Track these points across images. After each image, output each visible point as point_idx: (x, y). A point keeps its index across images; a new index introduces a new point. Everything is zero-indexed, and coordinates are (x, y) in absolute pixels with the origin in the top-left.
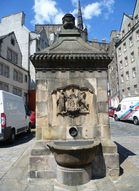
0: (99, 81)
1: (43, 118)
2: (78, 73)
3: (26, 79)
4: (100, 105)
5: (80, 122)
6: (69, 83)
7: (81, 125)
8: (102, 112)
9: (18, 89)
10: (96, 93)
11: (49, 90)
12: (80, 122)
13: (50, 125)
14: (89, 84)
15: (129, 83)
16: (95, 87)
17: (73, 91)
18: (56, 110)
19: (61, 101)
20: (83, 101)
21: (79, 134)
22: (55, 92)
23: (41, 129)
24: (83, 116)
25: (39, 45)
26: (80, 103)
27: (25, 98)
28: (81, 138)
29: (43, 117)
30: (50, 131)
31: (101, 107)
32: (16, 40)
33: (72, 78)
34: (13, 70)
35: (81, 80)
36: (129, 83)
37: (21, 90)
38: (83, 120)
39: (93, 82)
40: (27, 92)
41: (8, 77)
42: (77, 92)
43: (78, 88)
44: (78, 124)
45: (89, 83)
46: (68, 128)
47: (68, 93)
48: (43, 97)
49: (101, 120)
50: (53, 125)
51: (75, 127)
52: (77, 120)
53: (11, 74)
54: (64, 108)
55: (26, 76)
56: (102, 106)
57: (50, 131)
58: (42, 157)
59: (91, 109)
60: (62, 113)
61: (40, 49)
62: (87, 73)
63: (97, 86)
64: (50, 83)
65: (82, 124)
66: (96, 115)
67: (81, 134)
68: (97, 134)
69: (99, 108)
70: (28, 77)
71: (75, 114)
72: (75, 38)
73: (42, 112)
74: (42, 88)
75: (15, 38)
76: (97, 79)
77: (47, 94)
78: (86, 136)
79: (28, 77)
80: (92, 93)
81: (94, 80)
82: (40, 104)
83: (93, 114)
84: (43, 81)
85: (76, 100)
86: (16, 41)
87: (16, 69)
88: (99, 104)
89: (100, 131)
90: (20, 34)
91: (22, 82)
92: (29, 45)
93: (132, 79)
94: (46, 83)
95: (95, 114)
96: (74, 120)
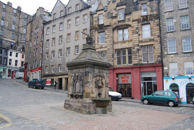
2: (101, 70)
6: (98, 74)
15: (54, 61)
18: (94, 86)
26: (102, 83)
28: (101, 97)
33: (99, 72)
36: (54, 61)
44: (100, 91)
48: (90, 80)
59: (104, 86)
72: (94, 51)
93: (57, 58)
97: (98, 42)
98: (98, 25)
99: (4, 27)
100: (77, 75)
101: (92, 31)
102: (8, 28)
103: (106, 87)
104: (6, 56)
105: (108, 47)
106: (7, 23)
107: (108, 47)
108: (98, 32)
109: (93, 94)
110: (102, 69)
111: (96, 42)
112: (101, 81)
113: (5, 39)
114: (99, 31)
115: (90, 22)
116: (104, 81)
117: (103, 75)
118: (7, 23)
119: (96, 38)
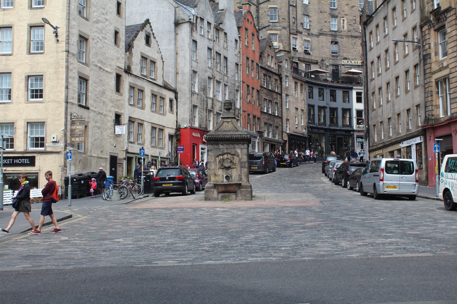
3: (171, 106)
5: (231, 172)
6: (226, 151)
8: (243, 167)
9: (158, 127)
10: (240, 157)
13: (215, 174)
16: (240, 154)
17: (228, 155)
18: (218, 166)
19: (222, 161)
20: (233, 161)
21: (231, 179)
22: (218, 156)
23: (210, 176)
24: (233, 169)
25: (194, 34)
27: (170, 143)
30: (215, 178)
31: (243, 165)
32: (153, 34)
34: (150, 94)
37: (162, 130)
38: (232, 172)
39: (239, 151)
40: (173, 132)
41: (143, 108)
42: (229, 156)
43: (230, 154)
46: (225, 176)
47: (225, 156)
49: (243, 172)
50: (217, 174)
52: (229, 171)
53: (148, 101)
54: (222, 165)
55: (171, 101)
58: (211, 190)
60: (222, 167)
61: (197, 40)
62: (236, 146)
63: (241, 153)
67: (232, 179)
68: (241, 179)
70: (175, 101)
71: (229, 168)
72: (230, 120)
75: (152, 30)
76: (241, 149)
77: (213, 158)
79: (175, 101)
80: (238, 157)
84: (211, 150)
85: (229, 161)
86: (152, 36)
87: (154, 90)
90: (155, 11)
91: (164, 114)
92: (176, 34)
97: (436, 54)
98: (431, 13)
99: (338, 33)
101: (424, 29)
102: (350, 34)
103: (241, 167)
104: (346, 106)
105: (451, 66)
106: (346, 22)
107: (451, 66)
108: (435, 31)
109: (217, 178)
110: (232, 144)
111: (433, 55)
113: (345, 62)
114: (437, 27)
115: (420, 7)
116: (236, 160)
117: (236, 152)
118: (346, 22)
119: (432, 46)
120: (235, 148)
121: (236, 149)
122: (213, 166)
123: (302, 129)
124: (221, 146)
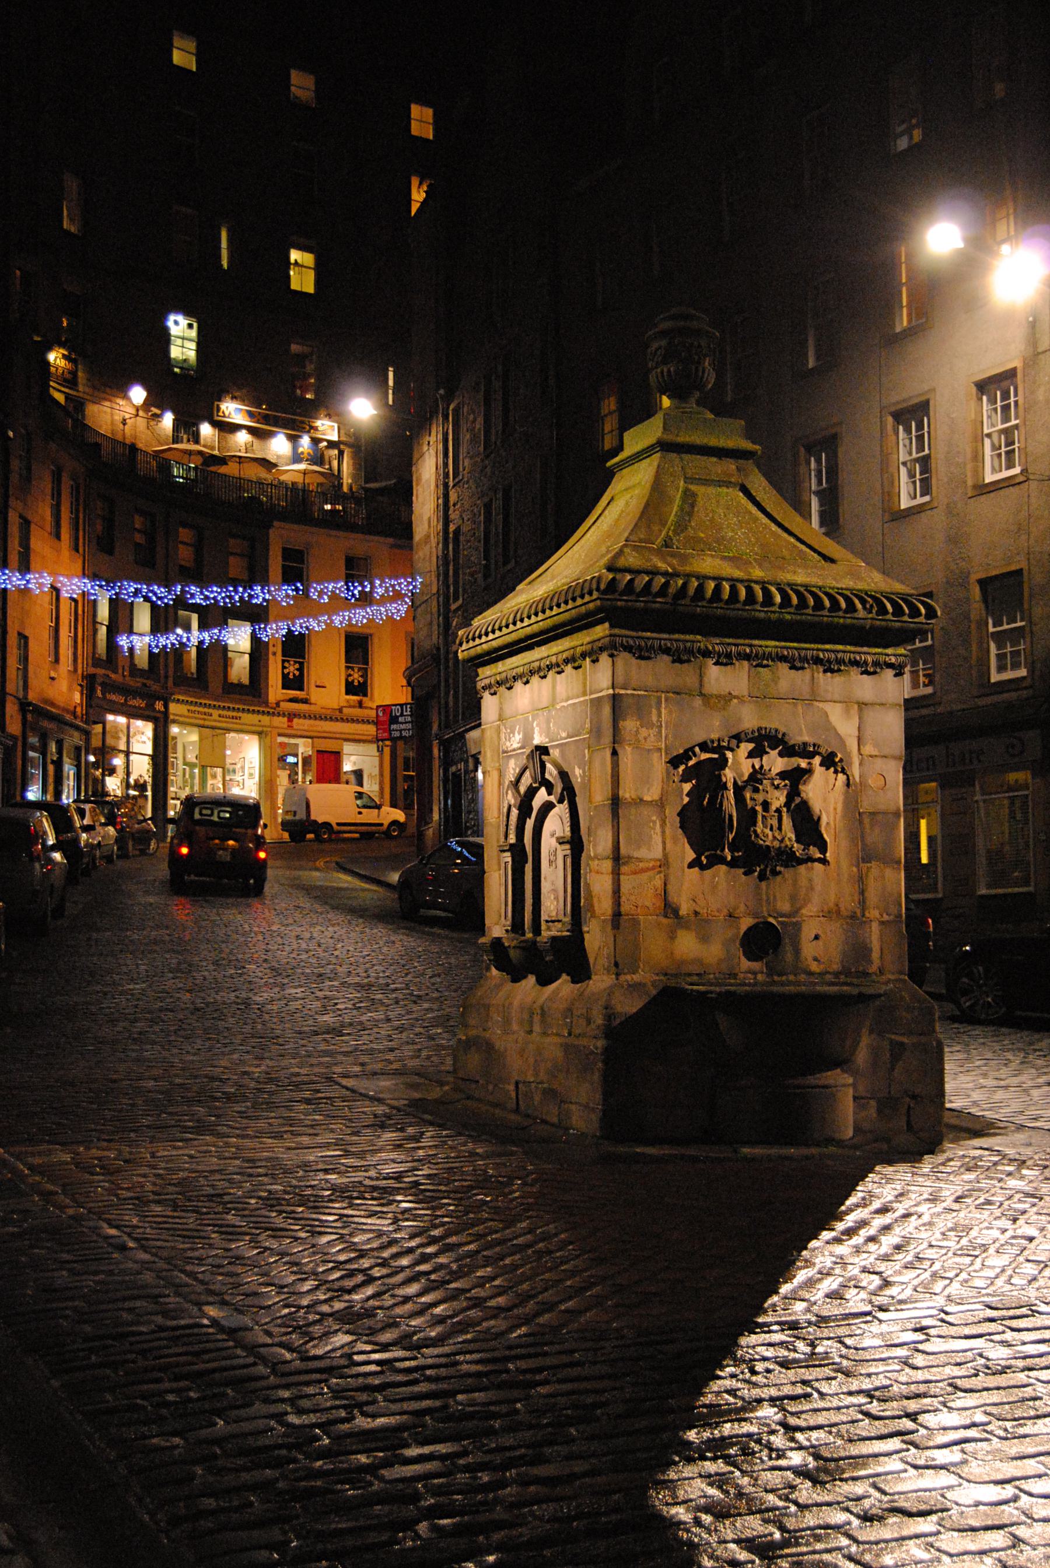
0: (870, 715)
1: (645, 876)
2: (787, 679)
4: (872, 826)
6: (749, 719)
7: (795, 912)
10: (855, 771)
11: (666, 746)
12: (793, 898)
14: (829, 727)
24: (802, 869)
29: (644, 871)
31: (874, 836)
35: (800, 707)
44: (785, 907)
45: (830, 723)
48: (644, 779)
51: (771, 920)
56: (877, 831)
57: (672, 937)
64: (670, 712)
65: (800, 909)
66: (855, 869)
67: (797, 951)
69: (869, 840)
73: (639, 847)
74: (641, 737)
78: (815, 959)
81: (852, 712)
82: (633, 811)
83: (845, 864)
88: (866, 820)
89: (868, 941)
94: (654, 711)
95: (852, 865)
96: (767, 889)
100: (537, 740)
112: (778, 799)
120: (814, 697)
121: (828, 707)
122: (657, 839)
123: (70, 689)
124: (716, 676)
